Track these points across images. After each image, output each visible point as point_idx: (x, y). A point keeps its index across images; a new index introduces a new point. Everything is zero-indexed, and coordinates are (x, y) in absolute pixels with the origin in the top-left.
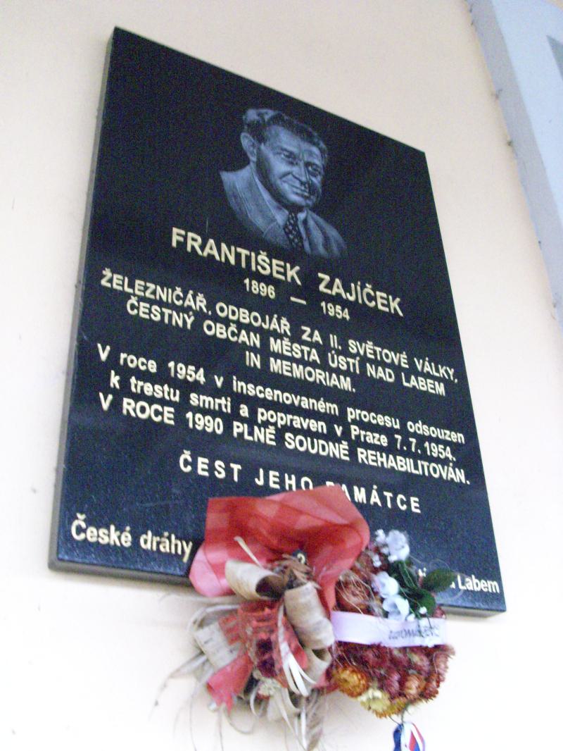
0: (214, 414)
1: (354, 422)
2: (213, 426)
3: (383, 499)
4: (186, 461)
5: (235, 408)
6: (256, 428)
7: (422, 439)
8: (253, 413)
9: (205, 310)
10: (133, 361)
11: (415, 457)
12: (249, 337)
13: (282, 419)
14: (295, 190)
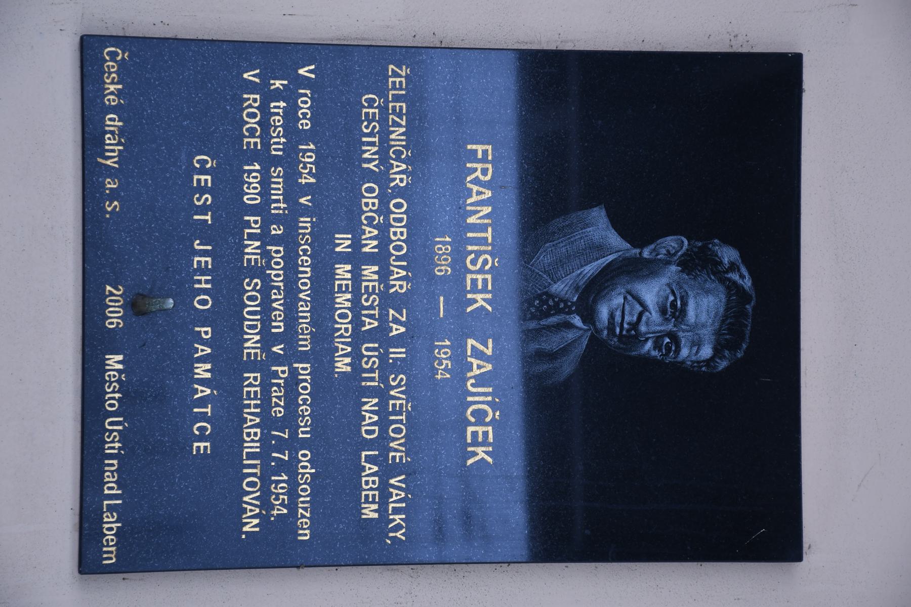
0: (265, 192)
1: (294, 373)
2: (251, 196)
3: (203, 402)
4: (206, 162)
5: (277, 219)
6: (257, 244)
7: (291, 468)
8: (276, 240)
9: (392, 184)
10: (305, 106)
11: (263, 455)
12: (370, 238)
13: (277, 275)
14: (618, 314)
